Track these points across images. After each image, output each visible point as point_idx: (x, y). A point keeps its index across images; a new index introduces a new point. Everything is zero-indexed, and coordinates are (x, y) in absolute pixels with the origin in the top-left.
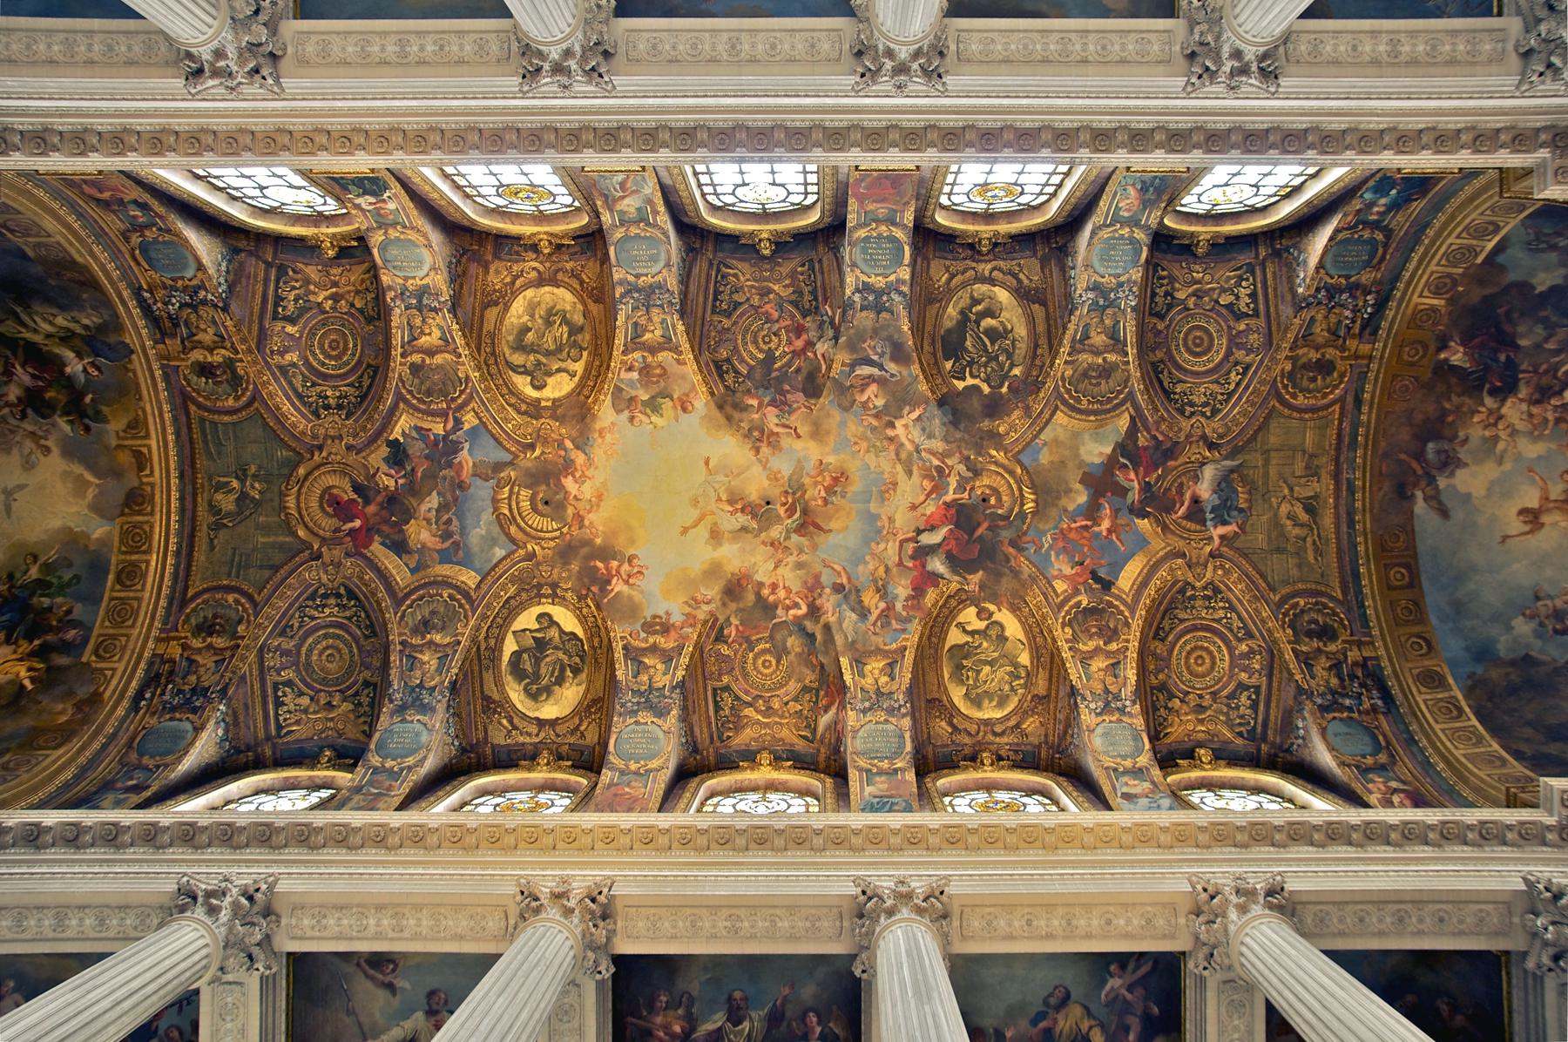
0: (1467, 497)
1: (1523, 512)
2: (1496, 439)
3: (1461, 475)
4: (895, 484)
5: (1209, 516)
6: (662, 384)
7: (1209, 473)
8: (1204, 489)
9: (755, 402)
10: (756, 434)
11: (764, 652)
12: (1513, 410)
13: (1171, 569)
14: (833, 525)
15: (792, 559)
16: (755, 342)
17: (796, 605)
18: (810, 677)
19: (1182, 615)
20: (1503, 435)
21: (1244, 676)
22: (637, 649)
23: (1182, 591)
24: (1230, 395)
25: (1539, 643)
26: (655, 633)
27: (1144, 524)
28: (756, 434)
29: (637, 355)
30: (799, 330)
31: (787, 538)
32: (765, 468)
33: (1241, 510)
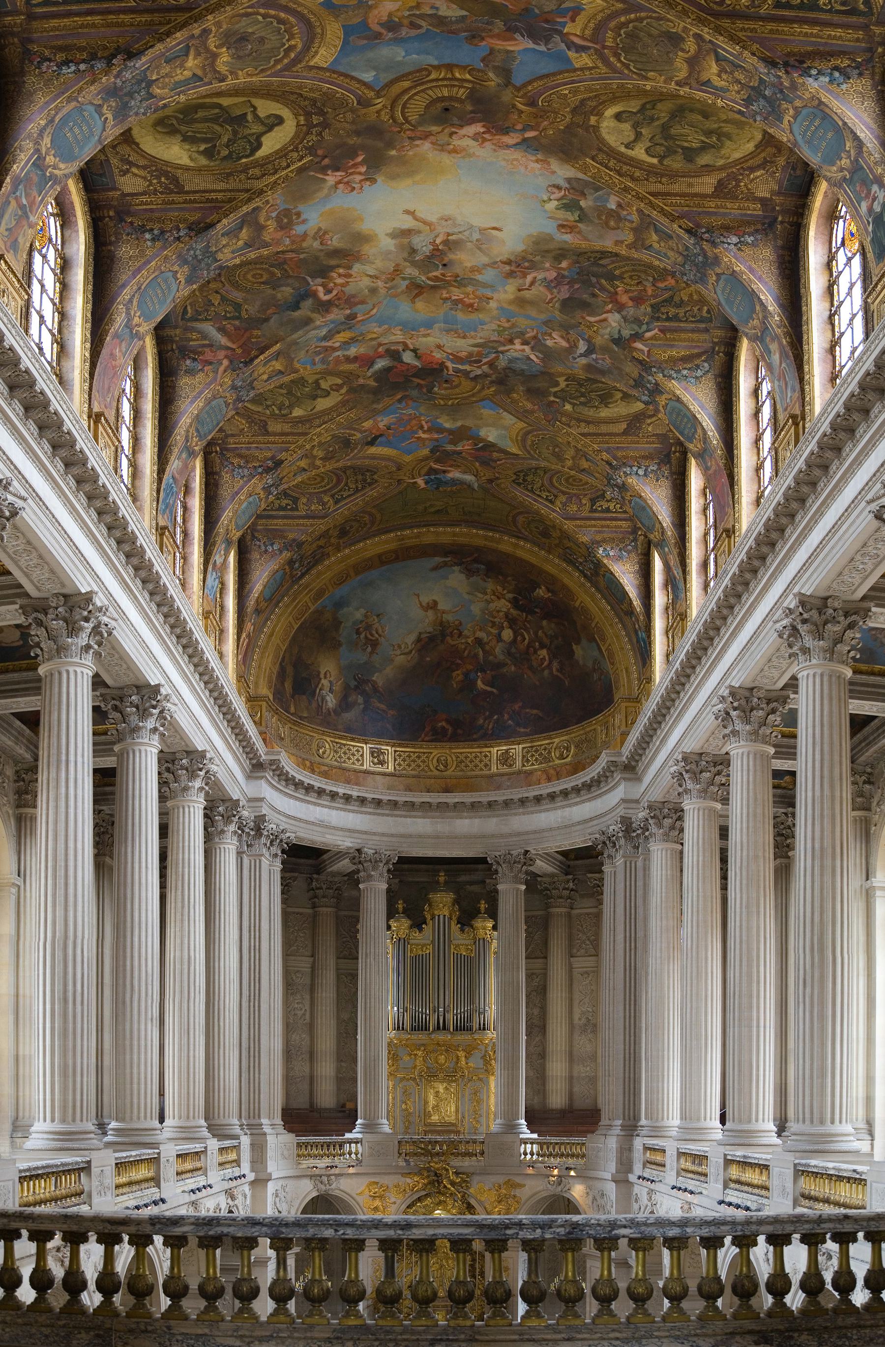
4: (464, 337)
5: (433, 477)
6: (597, 221)
7: (469, 478)
8: (455, 474)
9: (564, 264)
10: (526, 264)
11: (273, 274)
13: (386, 467)
14: (420, 304)
15: (380, 284)
16: (633, 270)
17: (328, 291)
18: (251, 309)
19: (348, 472)
21: (305, 500)
22: (256, 218)
23: (368, 471)
24: (532, 491)
26: (278, 219)
27: (426, 452)
28: (526, 264)
29: (635, 217)
30: (638, 300)
31: (404, 279)
32: (488, 265)
33: (437, 488)
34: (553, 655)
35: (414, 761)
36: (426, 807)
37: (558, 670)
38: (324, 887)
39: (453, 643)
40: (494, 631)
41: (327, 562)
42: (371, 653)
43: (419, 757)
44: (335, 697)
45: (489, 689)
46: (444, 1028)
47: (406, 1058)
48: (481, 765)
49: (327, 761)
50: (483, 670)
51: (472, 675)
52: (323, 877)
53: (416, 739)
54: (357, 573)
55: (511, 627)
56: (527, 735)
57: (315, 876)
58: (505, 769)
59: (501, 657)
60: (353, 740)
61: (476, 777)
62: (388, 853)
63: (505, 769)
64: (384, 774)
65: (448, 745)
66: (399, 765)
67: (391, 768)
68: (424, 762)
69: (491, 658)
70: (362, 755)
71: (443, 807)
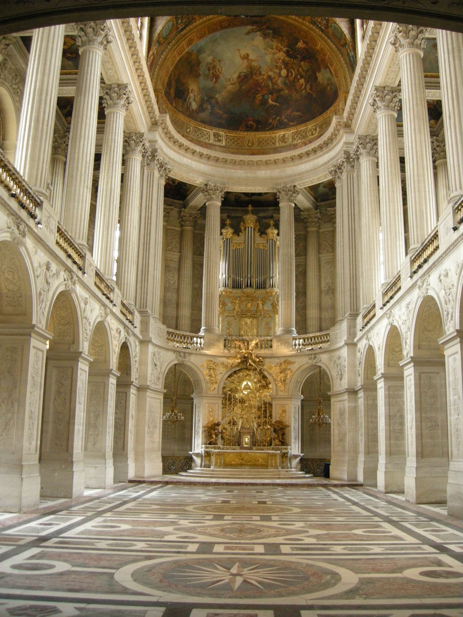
0: (253, 39)
1: (248, 55)
2: (272, 49)
3: (261, 38)
12: (281, 55)
20: (274, 51)
25: (204, 64)
34: (307, 82)
35: (236, 141)
36: (242, 163)
37: (310, 90)
38: (187, 216)
39: (256, 78)
40: (277, 71)
41: (194, 24)
42: (216, 82)
43: (239, 139)
44: (196, 104)
45: (274, 103)
46: (251, 286)
47: (230, 305)
48: (271, 143)
49: (191, 136)
50: (272, 94)
51: (266, 97)
52: (187, 210)
53: (237, 130)
54: (210, 33)
55: (285, 68)
56: (294, 126)
57: (183, 209)
58: (283, 144)
59: (281, 86)
60: (205, 127)
61: (268, 149)
62: (222, 186)
63: (283, 144)
64: (220, 146)
65: (253, 133)
66: (229, 143)
67: (224, 144)
68: (241, 142)
69: (276, 86)
70: (209, 136)
71: (250, 164)
